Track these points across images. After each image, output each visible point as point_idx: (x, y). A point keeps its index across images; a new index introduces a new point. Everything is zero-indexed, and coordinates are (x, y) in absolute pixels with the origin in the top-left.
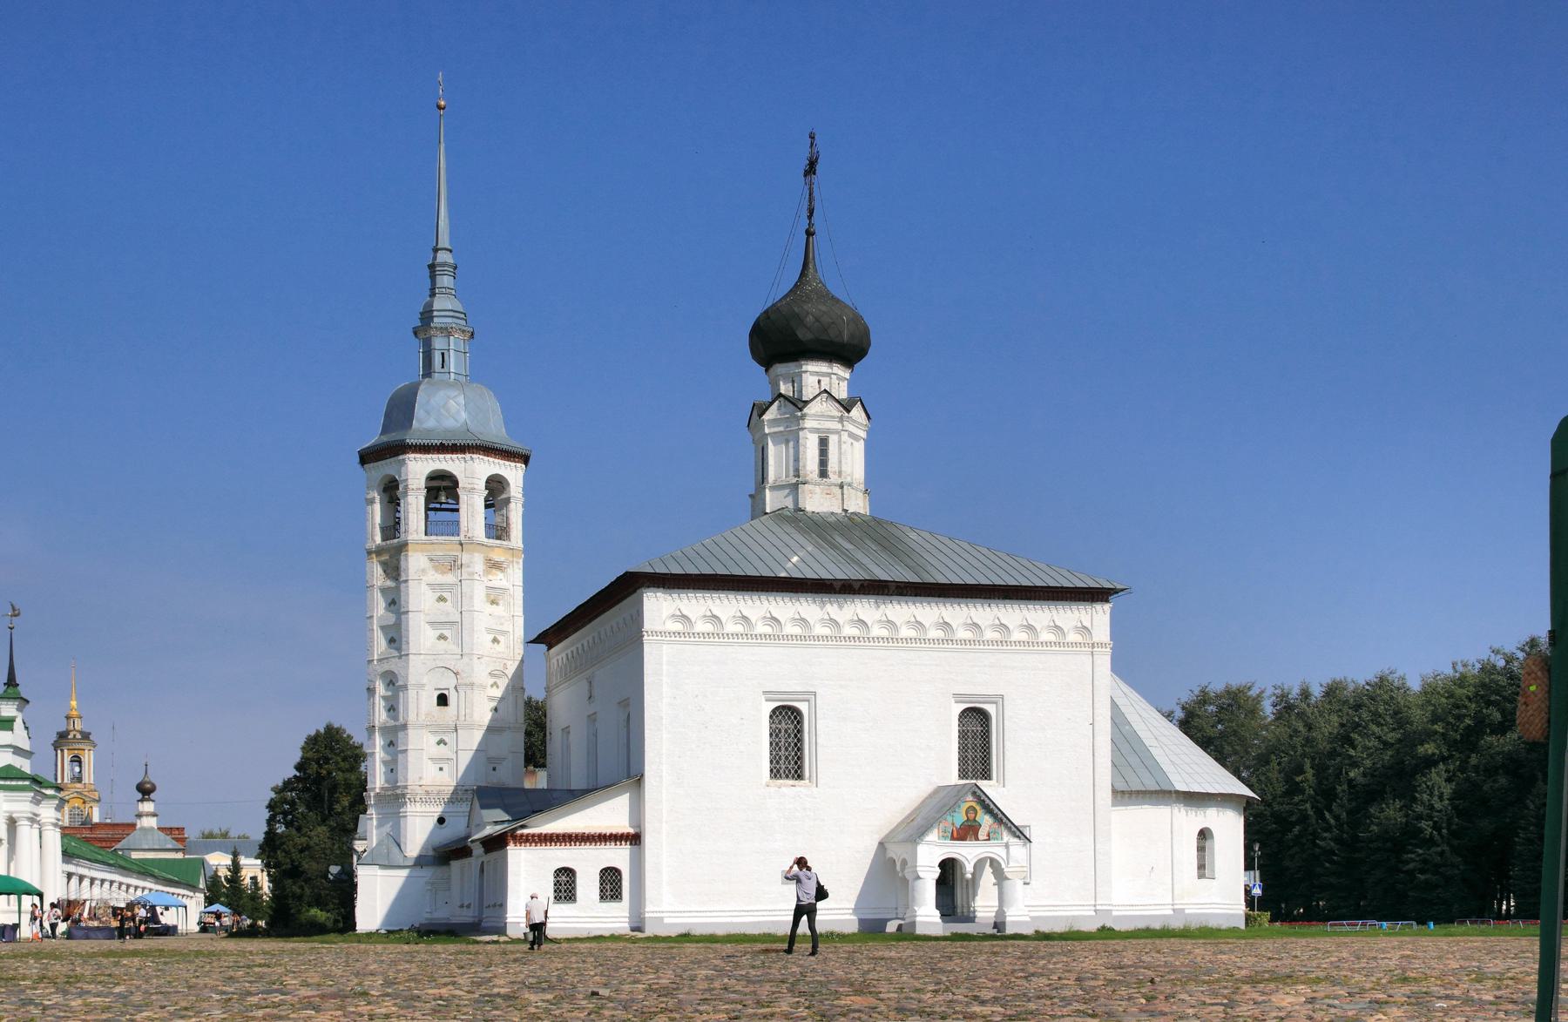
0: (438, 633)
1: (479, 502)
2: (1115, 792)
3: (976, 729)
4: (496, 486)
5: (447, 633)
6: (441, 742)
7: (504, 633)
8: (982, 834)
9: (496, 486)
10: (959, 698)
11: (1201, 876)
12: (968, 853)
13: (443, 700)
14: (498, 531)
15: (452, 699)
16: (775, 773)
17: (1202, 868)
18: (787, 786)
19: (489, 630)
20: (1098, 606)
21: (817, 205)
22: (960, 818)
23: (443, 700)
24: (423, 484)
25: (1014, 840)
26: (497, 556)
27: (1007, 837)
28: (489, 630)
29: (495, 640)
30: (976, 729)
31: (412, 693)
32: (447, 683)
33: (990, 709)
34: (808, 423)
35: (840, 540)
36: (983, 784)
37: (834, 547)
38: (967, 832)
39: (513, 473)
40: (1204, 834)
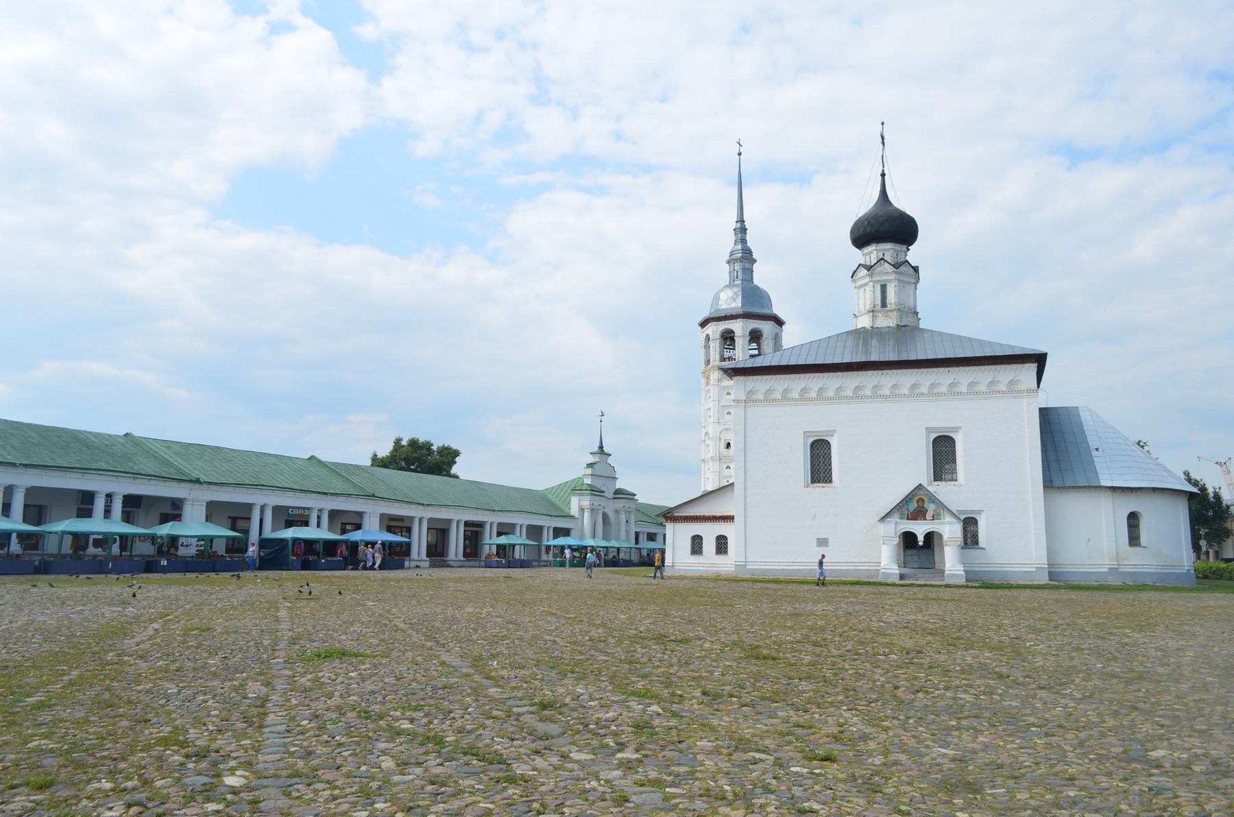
3: (943, 452)
8: (929, 516)
11: (1131, 544)
12: (920, 529)
16: (813, 481)
17: (1134, 540)
18: (820, 488)
20: (1027, 365)
22: (913, 506)
23: (728, 445)
24: (718, 336)
27: (948, 518)
30: (943, 452)
34: (876, 278)
35: (874, 342)
36: (925, 485)
37: (866, 344)
38: (919, 514)
39: (766, 327)
40: (1133, 518)
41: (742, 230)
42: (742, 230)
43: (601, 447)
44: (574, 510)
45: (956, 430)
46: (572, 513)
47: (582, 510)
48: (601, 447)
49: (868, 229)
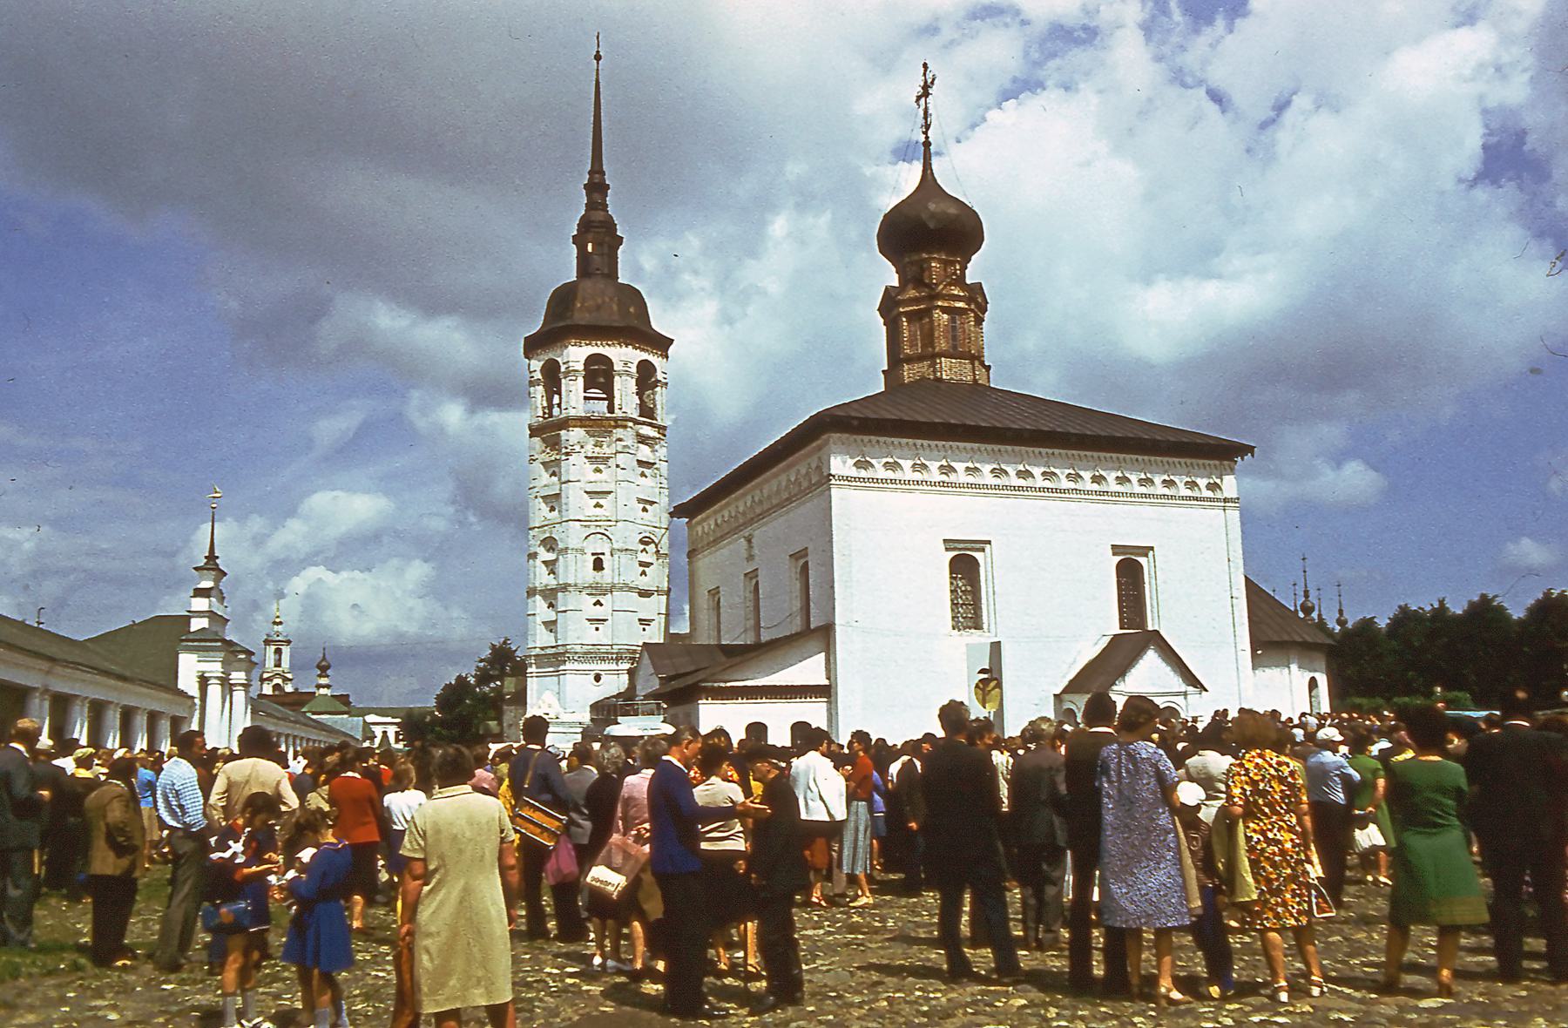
0: (594, 502)
1: (632, 385)
2: (1255, 644)
4: (646, 370)
5: (602, 502)
6: (598, 603)
7: (652, 503)
9: (646, 370)
10: (1116, 549)
13: (598, 565)
14: (647, 411)
15: (606, 559)
19: (640, 501)
21: (933, 120)
23: (598, 565)
25: (1191, 689)
26: (647, 431)
28: (640, 501)
29: (644, 510)
31: (570, 556)
32: (602, 546)
33: (1142, 560)
41: (597, 188)
42: (597, 188)
43: (212, 557)
44: (187, 682)
45: (1145, 551)
46: (181, 686)
47: (204, 681)
48: (212, 557)
49: (932, 225)
